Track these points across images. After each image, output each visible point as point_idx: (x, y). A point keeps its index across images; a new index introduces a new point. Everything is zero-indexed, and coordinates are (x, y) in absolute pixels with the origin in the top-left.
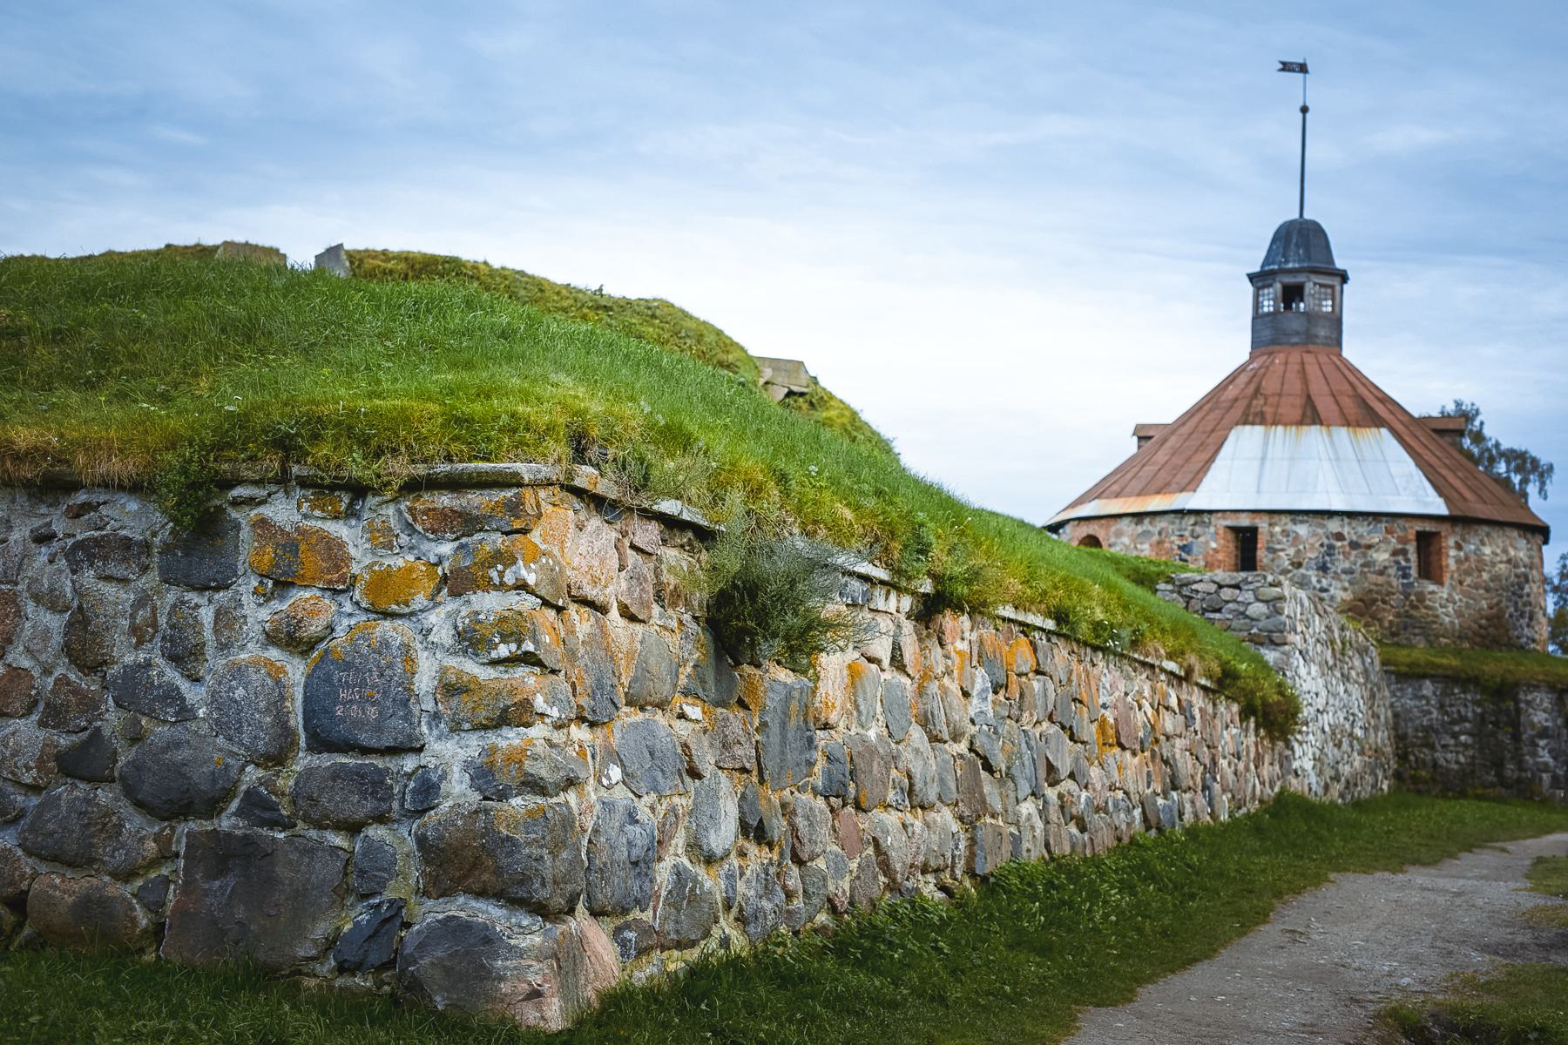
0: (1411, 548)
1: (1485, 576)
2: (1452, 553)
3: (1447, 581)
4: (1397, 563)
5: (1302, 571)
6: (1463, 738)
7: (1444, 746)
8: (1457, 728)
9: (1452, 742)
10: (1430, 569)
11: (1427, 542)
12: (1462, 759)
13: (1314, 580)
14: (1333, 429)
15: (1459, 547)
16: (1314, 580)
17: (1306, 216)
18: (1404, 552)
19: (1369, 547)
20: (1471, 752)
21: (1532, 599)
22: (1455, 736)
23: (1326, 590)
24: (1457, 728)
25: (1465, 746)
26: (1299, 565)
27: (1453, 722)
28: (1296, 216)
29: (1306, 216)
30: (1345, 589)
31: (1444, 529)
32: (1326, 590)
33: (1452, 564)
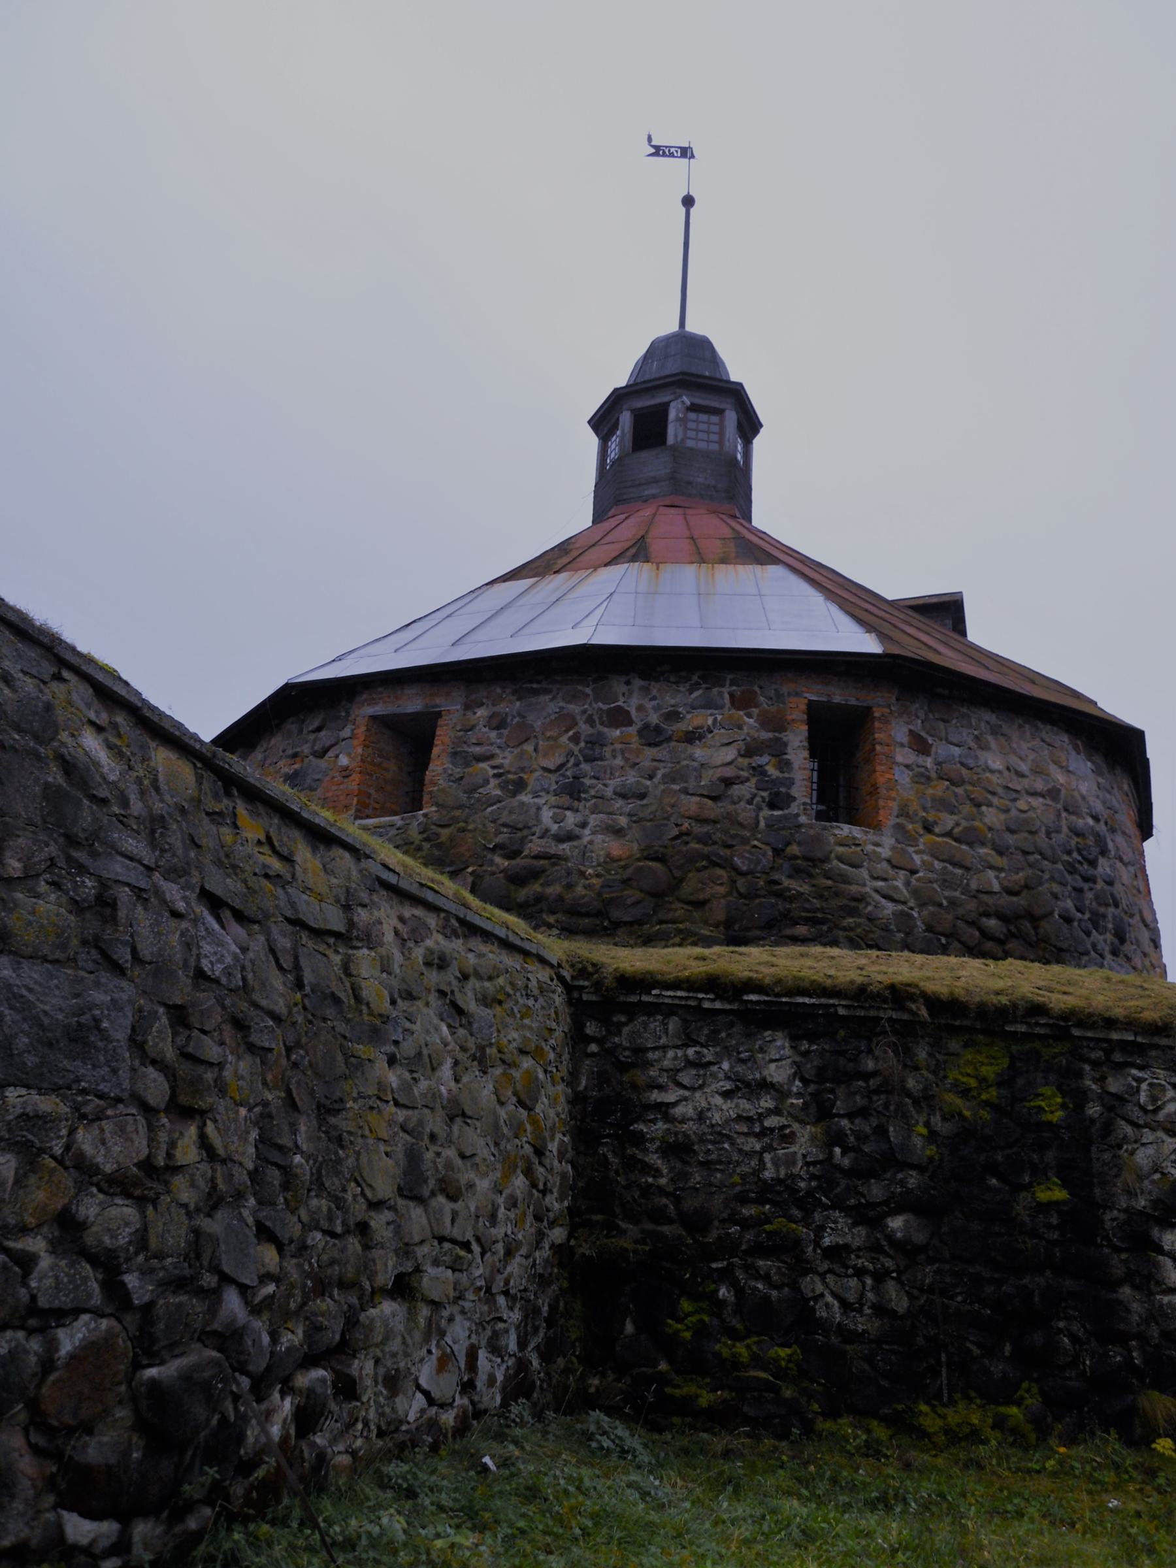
0: (797, 741)
1: (992, 817)
2: (904, 756)
3: (889, 816)
4: (759, 771)
5: (525, 798)
6: (896, 1223)
7: (836, 1253)
8: (876, 1191)
9: (857, 1237)
10: (842, 779)
11: (840, 746)
12: (898, 1300)
13: (547, 815)
14: (668, 569)
15: (920, 746)
16: (547, 815)
17: (689, 328)
18: (778, 750)
19: (691, 737)
20: (927, 1274)
21: (1118, 889)
22: (868, 1216)
23: (570, 837)
24: (876, 1191)
25: (903, 1248)
26: (520, 786)
27: (863, 1172)
28: (674, 327)
29: (689, 328)
30: (618, 832)
31: (881, 701)
32: (570, 837)
33: (903, 778)
